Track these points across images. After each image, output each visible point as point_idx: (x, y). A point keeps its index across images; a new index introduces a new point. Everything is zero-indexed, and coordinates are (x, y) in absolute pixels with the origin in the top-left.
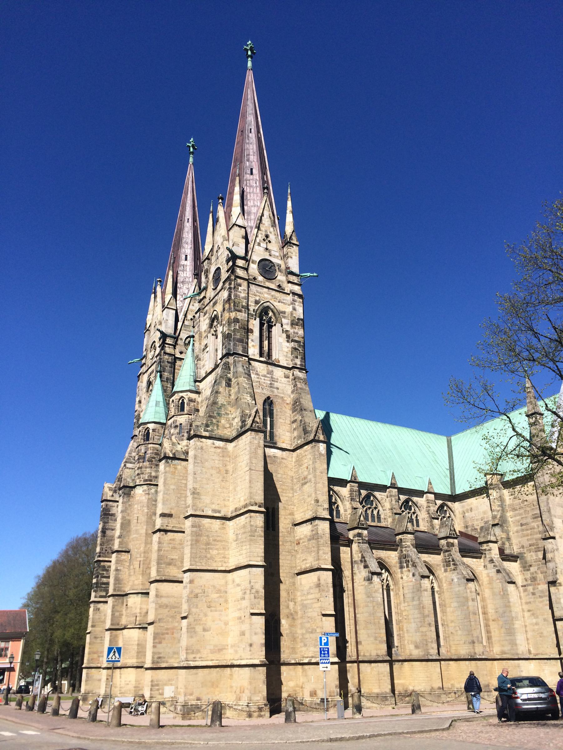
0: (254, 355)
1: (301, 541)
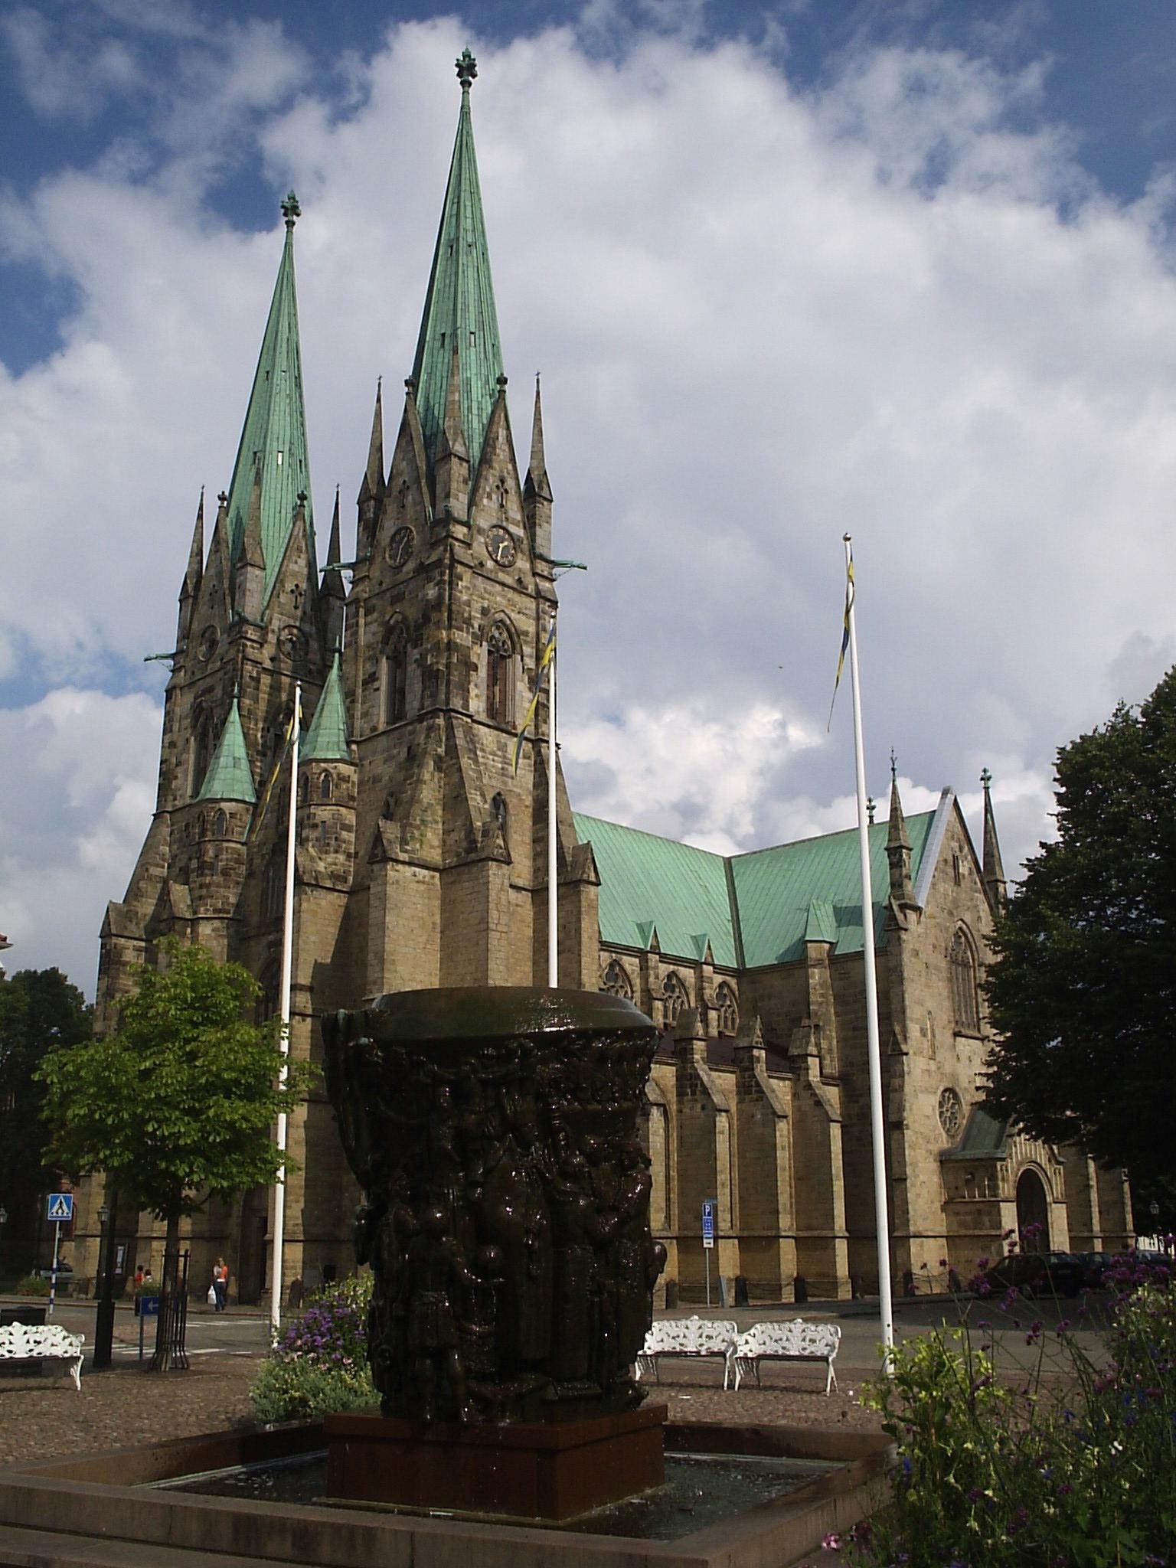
0: (478, 713)
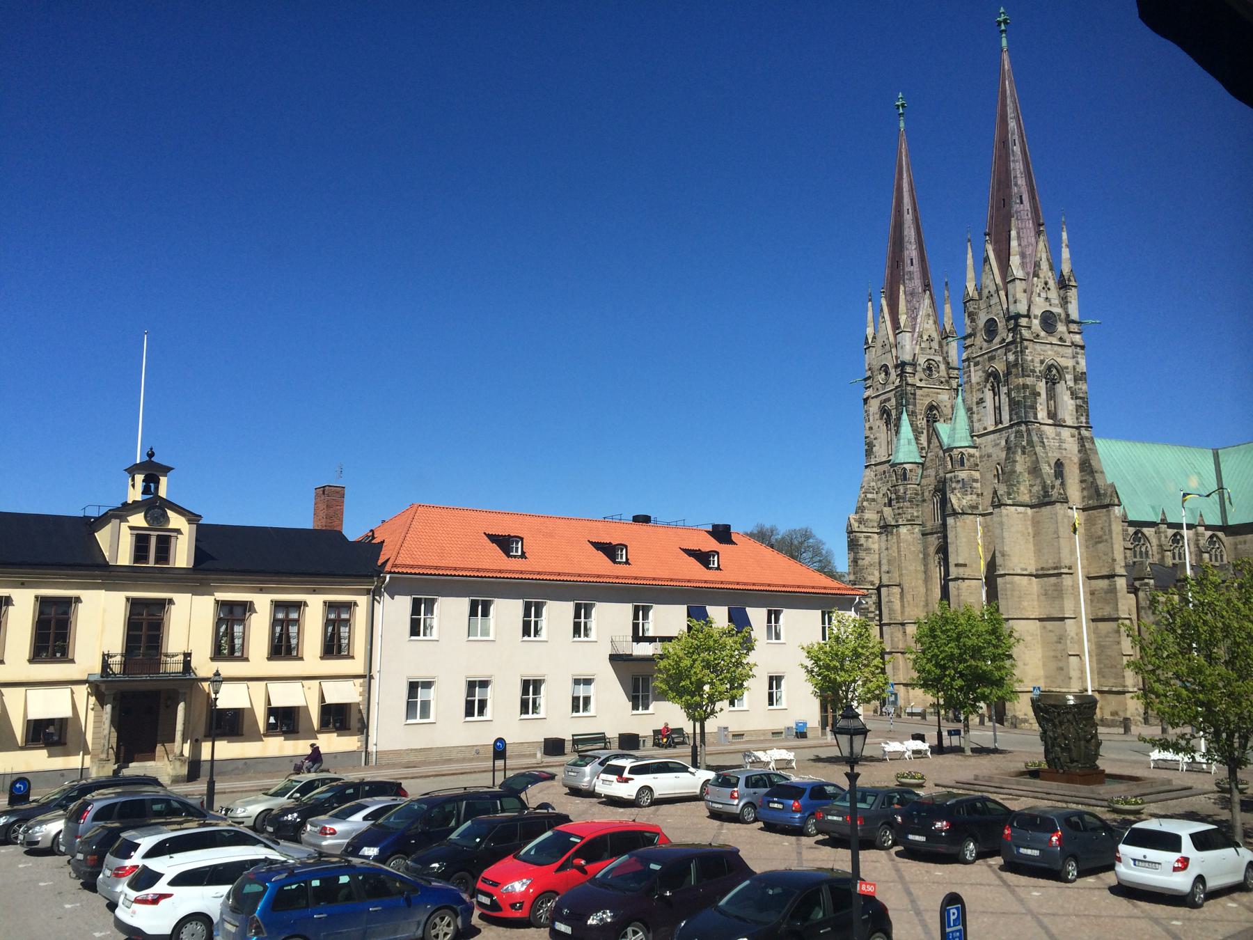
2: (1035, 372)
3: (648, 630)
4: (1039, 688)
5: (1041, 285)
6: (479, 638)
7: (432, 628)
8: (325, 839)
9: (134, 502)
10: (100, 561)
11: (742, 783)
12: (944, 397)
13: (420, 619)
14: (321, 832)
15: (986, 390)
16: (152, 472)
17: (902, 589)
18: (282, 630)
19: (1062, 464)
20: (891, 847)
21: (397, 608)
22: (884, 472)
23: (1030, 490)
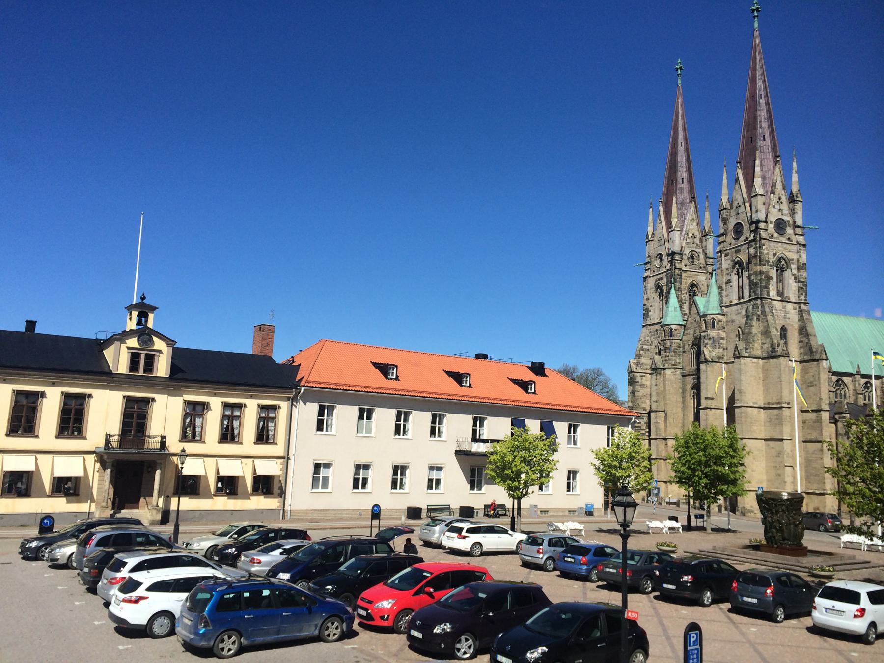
1: (807, 422)
2: (769, 262)
3: (483, 434)
4: (762, 488)
5: (776, 200)
6: (364, 434)
7: (331, 426)
8: (254, 566)
9: (131, 330)
10: (106, 370)
11: (546, 543)
12: (702, 279)
13: (324, 420)
14: (251, 562)
15: (733, 274)
16: (144, 309)
17: (666, 414)
18: (228, 423)
19: (785, 328)
20: (651, 592)
21: (308, 411)
22: (656, 330)
23: (762, 347)
